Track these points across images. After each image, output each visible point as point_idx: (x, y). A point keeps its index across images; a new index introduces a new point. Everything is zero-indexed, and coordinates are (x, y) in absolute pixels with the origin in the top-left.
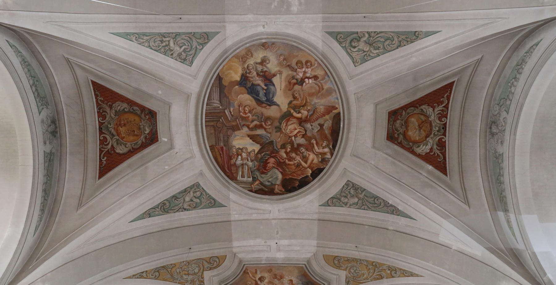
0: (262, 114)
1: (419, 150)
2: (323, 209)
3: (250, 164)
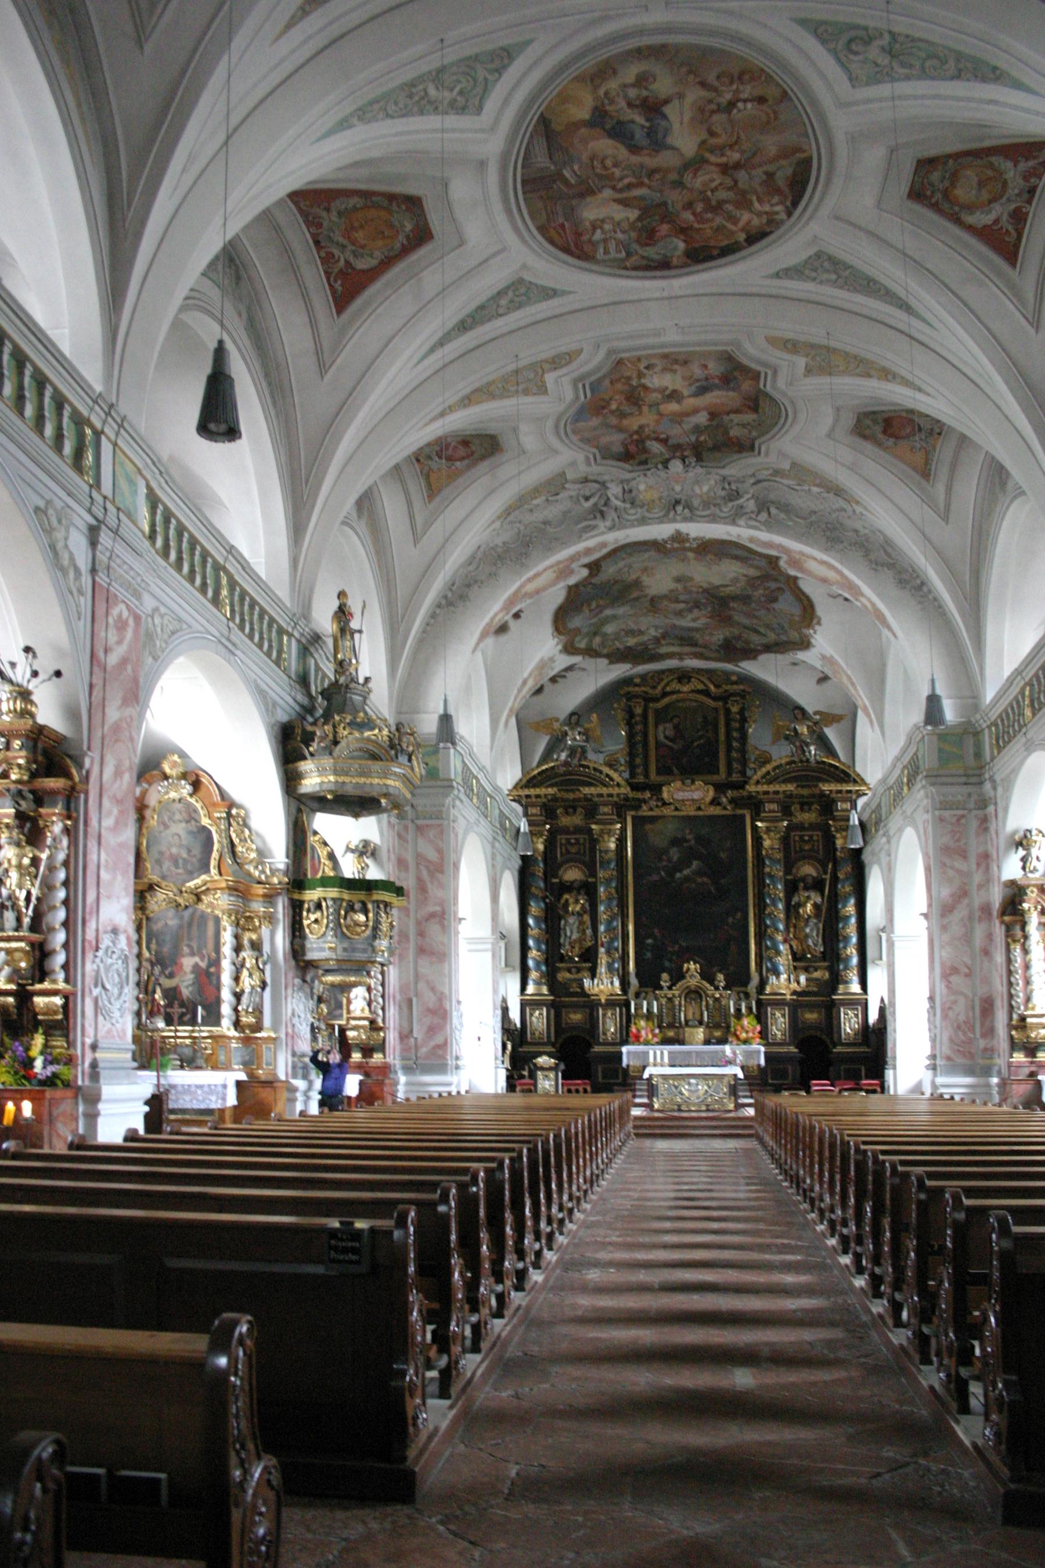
1: (970, 219)
3: (620, 236)
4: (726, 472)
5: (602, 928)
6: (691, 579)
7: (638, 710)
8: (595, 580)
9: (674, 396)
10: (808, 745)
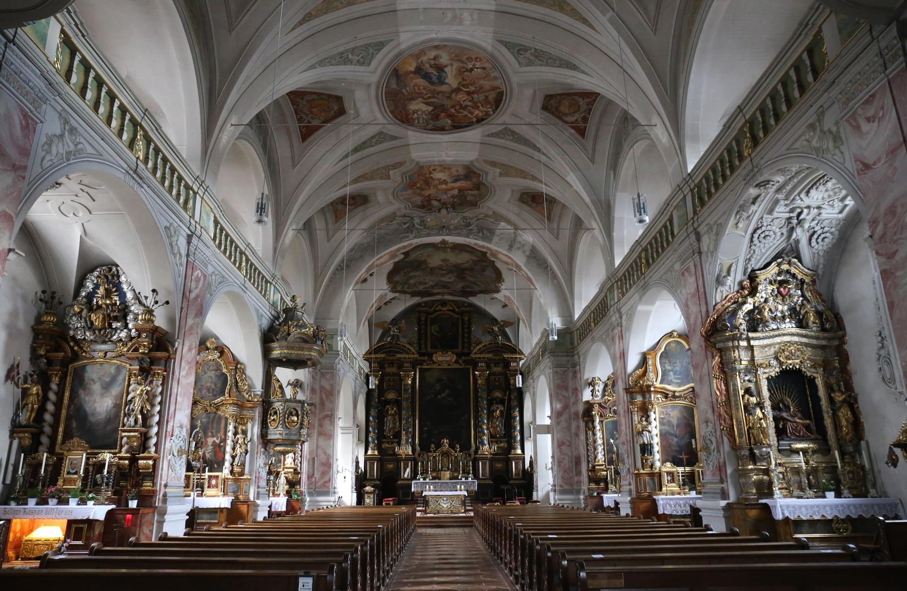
0: (435, 90)
2: (484, 138)
3: (425, 117)
4: (466, 214)
5: (403, 422)
6: (448, 260)
7: (423, 319)
8: (407, 260)
9: (445, 182)
10: (498, 336)
